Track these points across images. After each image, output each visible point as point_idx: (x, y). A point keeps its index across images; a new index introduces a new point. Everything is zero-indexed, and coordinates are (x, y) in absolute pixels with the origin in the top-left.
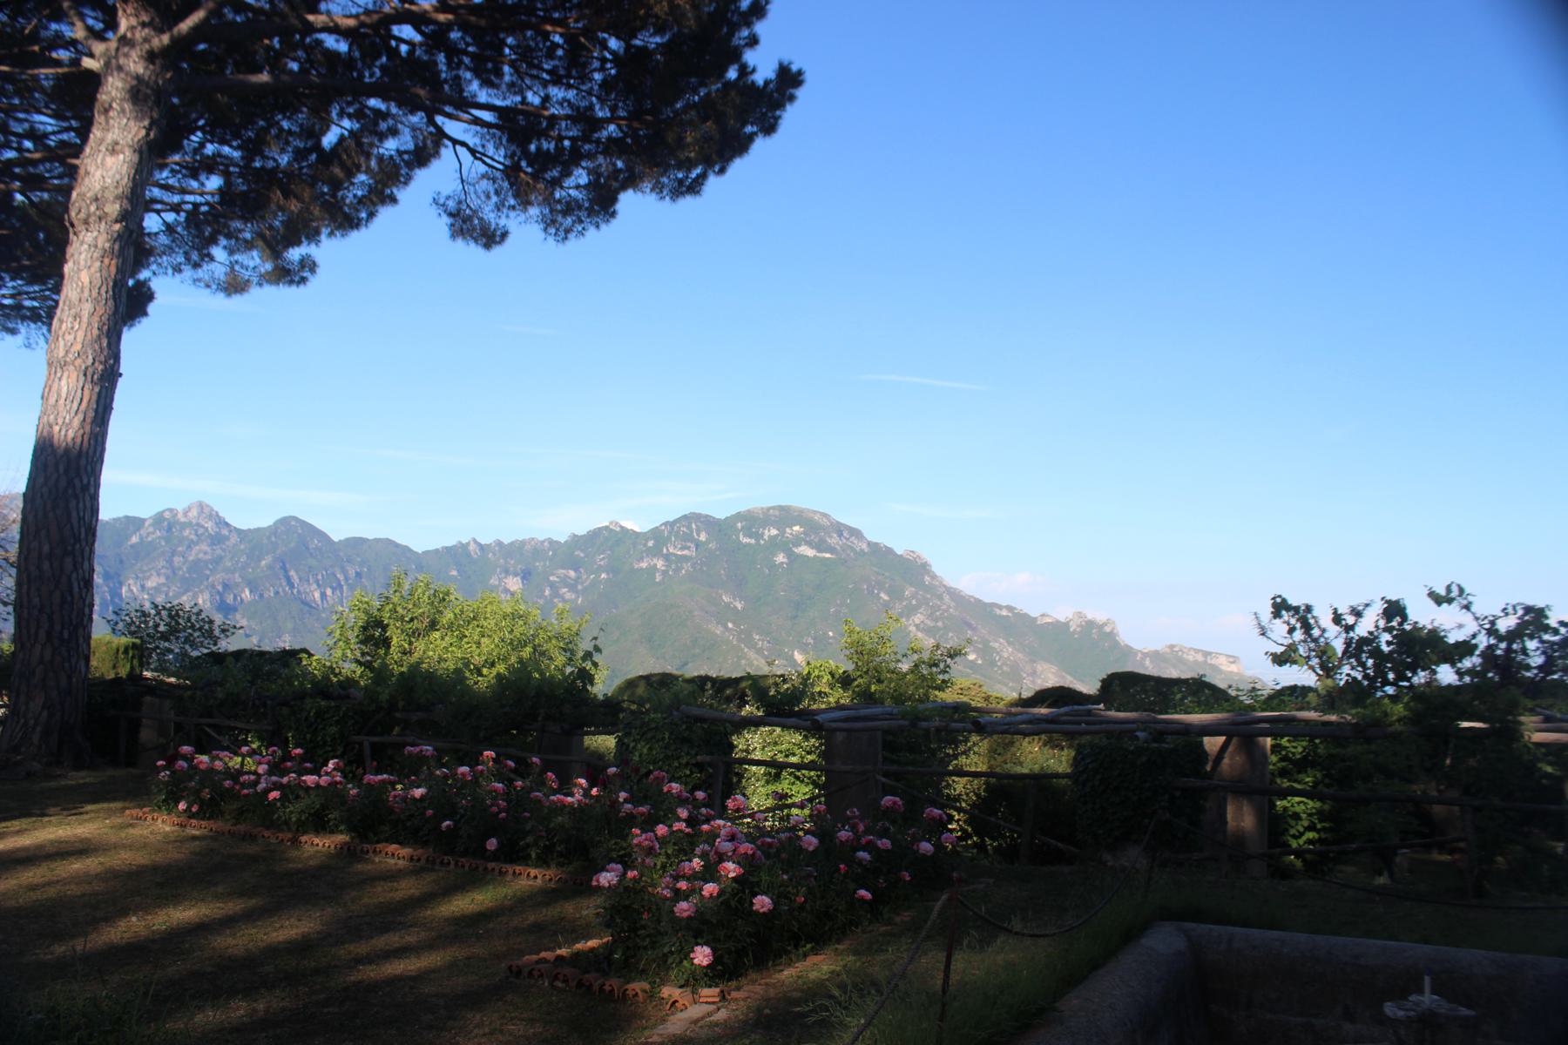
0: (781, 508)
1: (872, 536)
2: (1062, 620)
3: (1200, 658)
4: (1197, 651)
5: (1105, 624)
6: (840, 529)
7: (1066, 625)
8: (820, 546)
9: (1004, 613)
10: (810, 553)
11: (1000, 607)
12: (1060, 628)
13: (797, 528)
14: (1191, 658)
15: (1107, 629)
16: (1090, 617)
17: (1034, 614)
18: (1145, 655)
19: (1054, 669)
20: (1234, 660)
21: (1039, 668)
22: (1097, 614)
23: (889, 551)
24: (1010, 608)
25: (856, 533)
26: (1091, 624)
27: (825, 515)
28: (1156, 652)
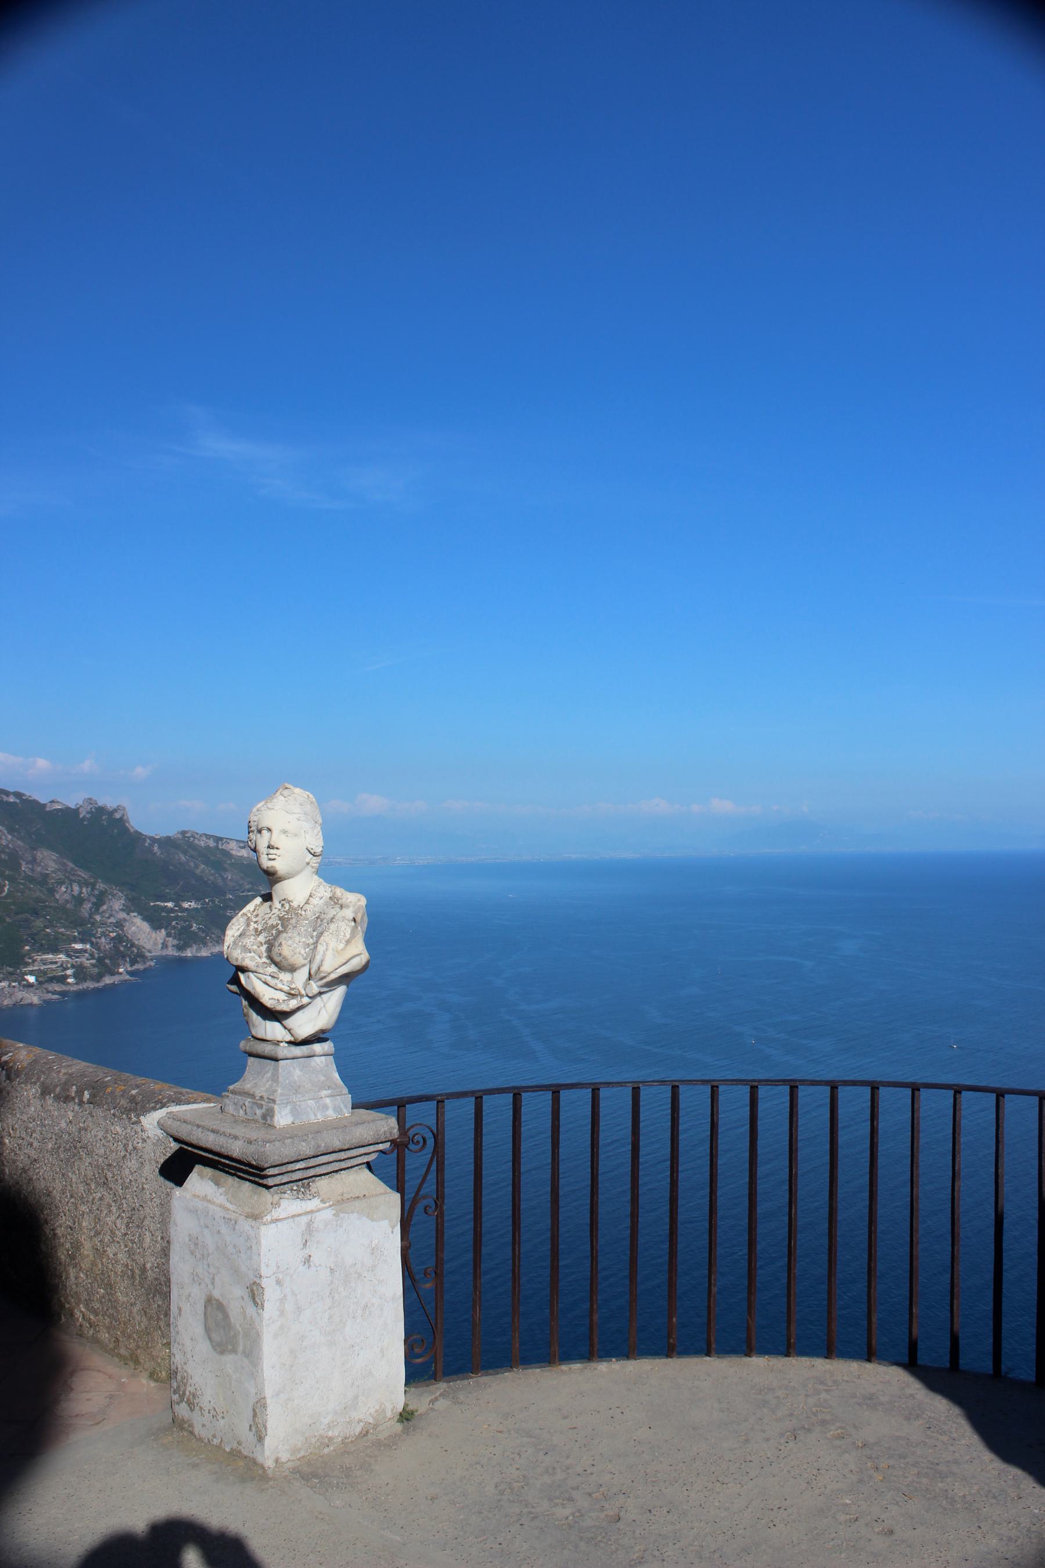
2: (73, 807)
3: (212, 843)
4: (208, 837)
5: (115, 811)
7: (76, 811)
9: (12, 799)
11: (7, 793)
12: (70, 814)
14: (202, 844)
15: (117, 816)
16: (100, 803)
17: (43, 801)
18: (154, 840)
19: (55, 856)
21: (39, 855)
22: (108, 801)
24: (18, 795)
26: (101, 810)
28: (169, 838)
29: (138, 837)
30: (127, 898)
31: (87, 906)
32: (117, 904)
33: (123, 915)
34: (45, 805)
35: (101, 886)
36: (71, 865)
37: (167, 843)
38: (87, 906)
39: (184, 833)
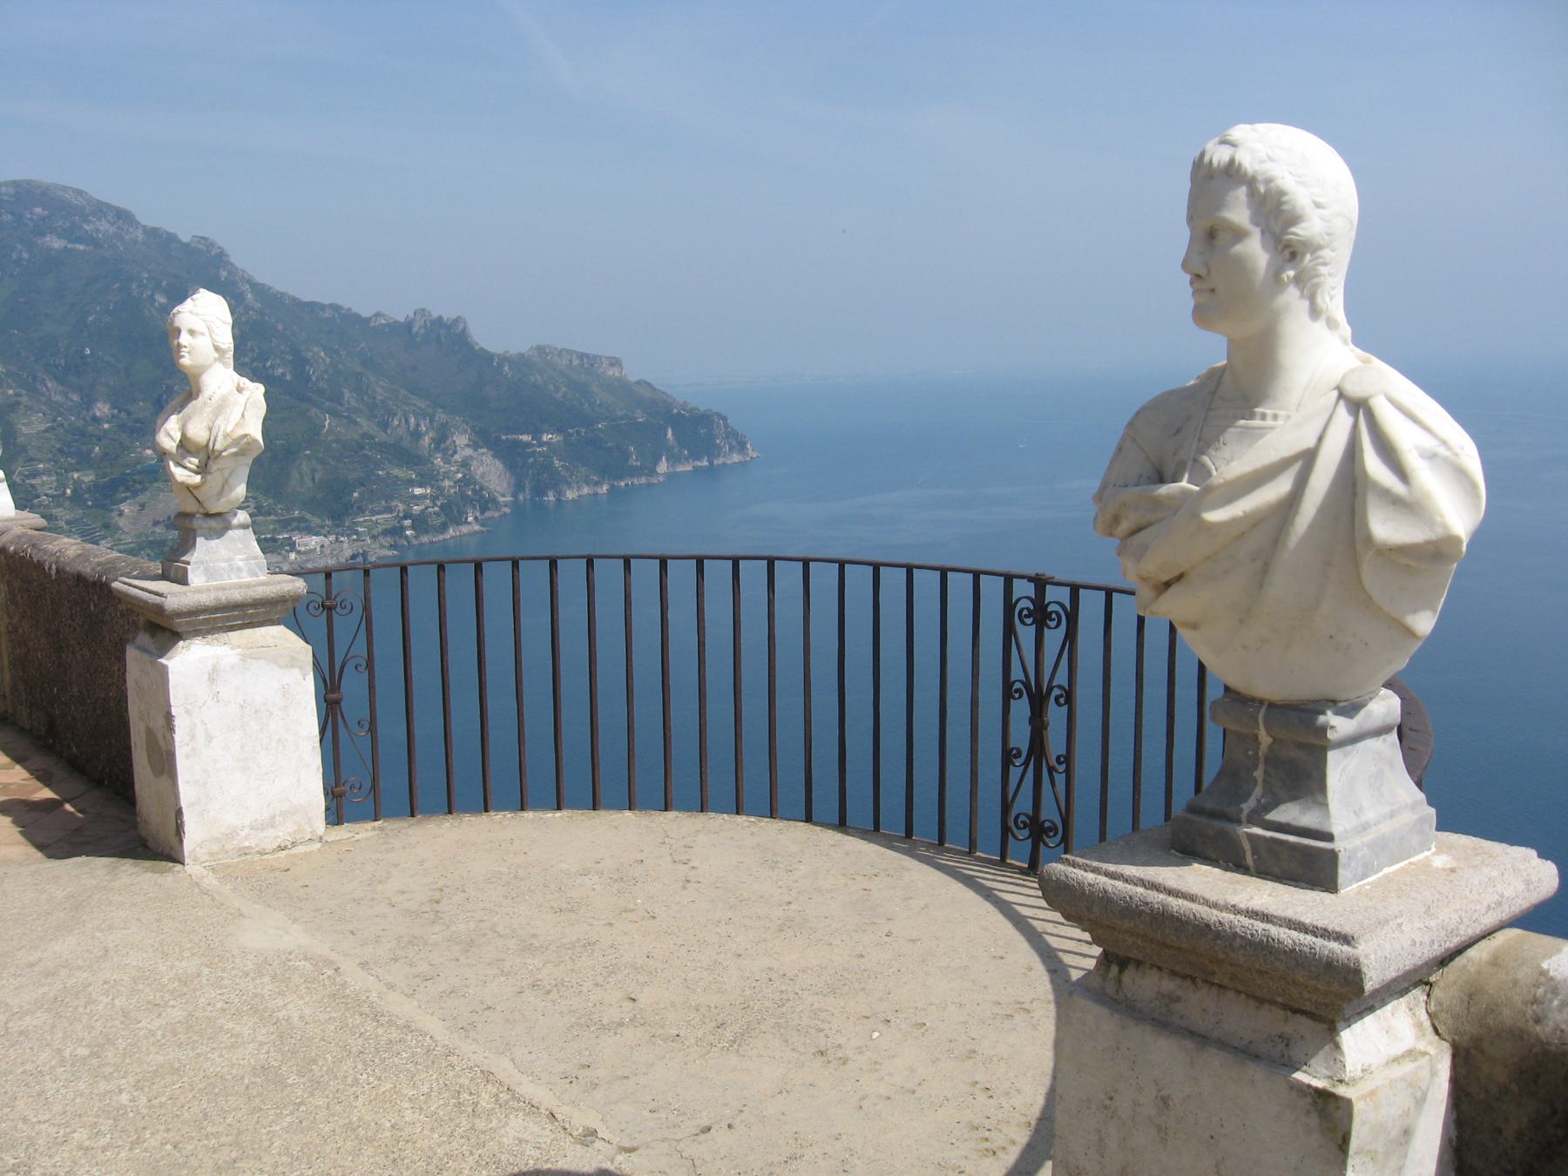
0: (16, 184)
1: (149, 216)
5: (457, 321)
6: (100, 209)
7: (409, 325)
8: (70, 234)
10: (58, 244)
11: (323, 307)
13: (38, 210)
18: (504, 359)
20: (615, 362)
22: (445, 310)
23: (172, 238)
25: (123, 216)
27: (79, 192)
28: (521, 356)
29: (486, 357)
30: (473, 429)
31: (426, 441)
32: (461, 440)
33: (469, 452)
34: (368, 320)
35: (441, 416)
36: (404, 392)
37: (521, 363)
38: (426, 441)
39: (541, 350)
